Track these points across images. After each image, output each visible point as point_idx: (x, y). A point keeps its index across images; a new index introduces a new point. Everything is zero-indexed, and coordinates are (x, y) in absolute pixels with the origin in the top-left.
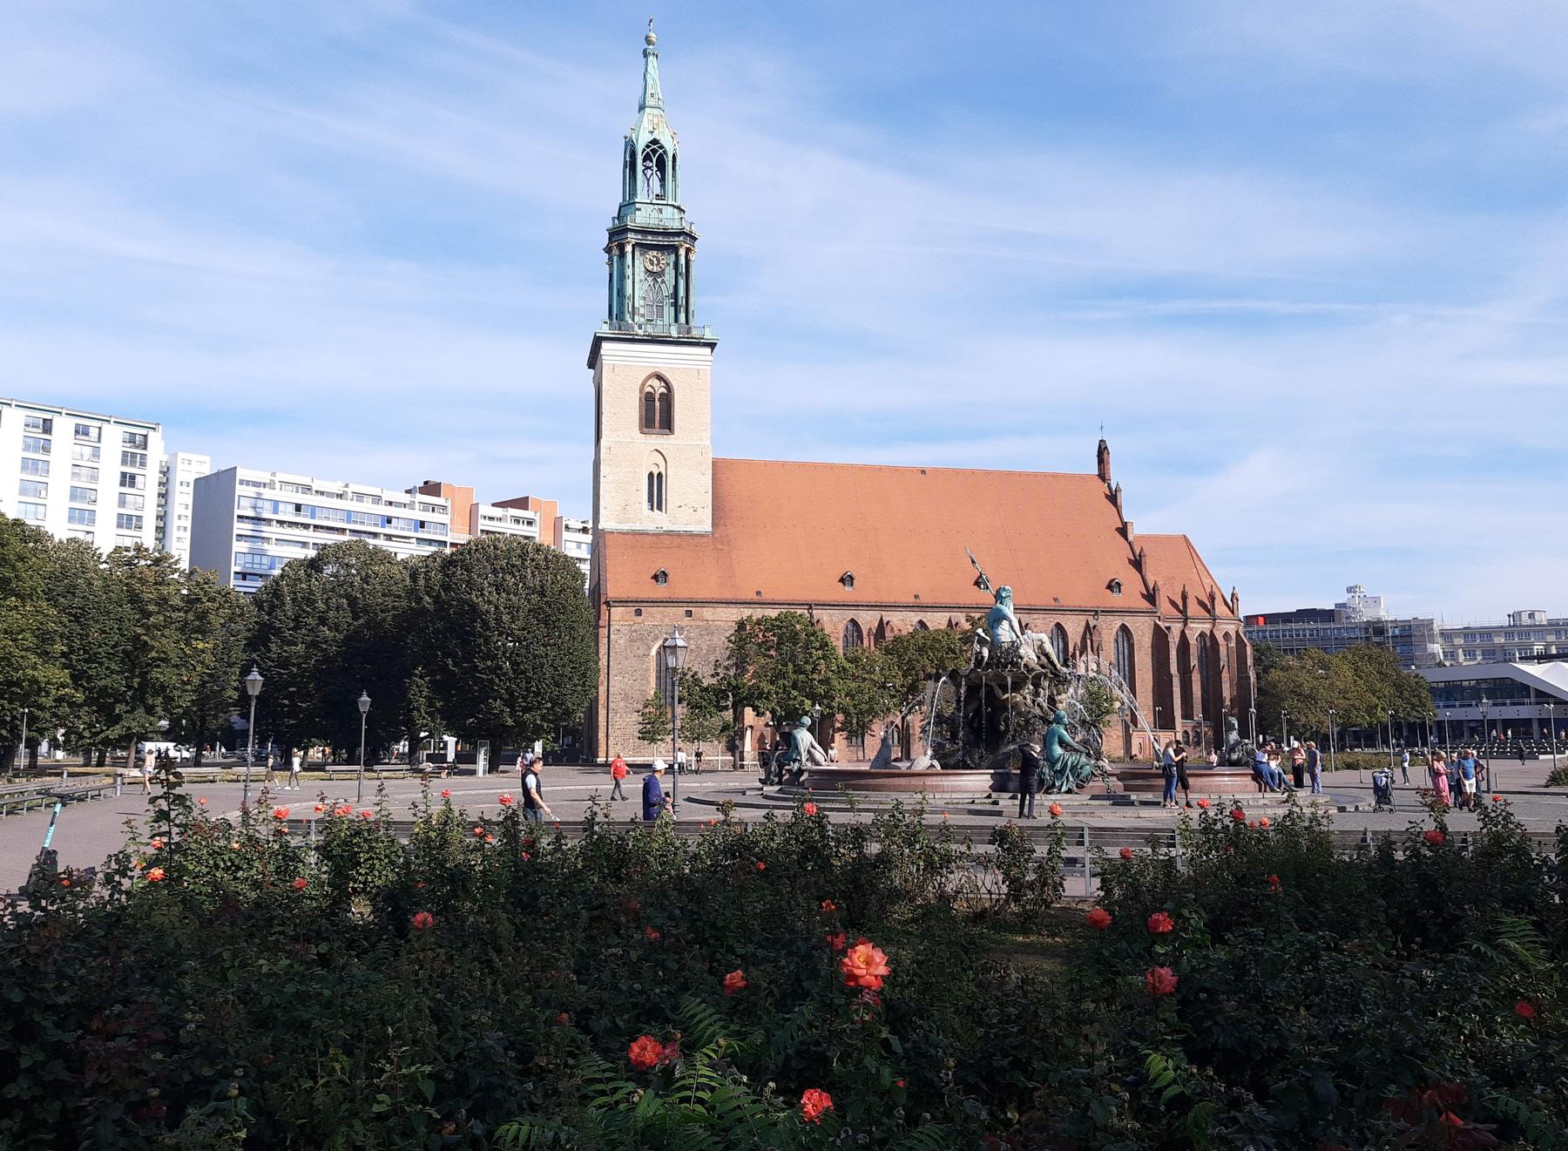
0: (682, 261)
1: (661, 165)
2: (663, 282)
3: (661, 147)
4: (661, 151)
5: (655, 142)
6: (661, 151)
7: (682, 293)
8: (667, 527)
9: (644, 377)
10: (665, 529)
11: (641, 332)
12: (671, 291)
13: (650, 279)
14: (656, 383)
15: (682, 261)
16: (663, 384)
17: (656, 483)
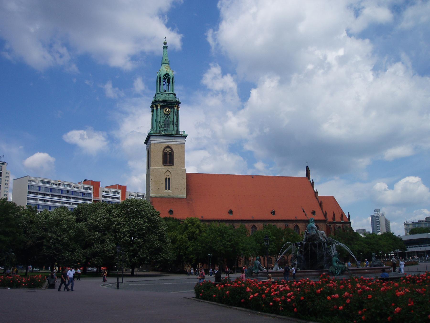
0: (176, 110)
1: (169, 82)
2: (170, 117)
3: (169, 76)
4: (169, 77)
5: (167, 74)
6: (169, 77)
7: (175, 121)
8: (172, 195)
9: (164, 147)
10: (171, 196)
11: (163, 133)
12: (172, 120)
13: (165, 116)
14: (168, 149)
15: (176, 110)
16: (170, 149)
17: (168, 180)
